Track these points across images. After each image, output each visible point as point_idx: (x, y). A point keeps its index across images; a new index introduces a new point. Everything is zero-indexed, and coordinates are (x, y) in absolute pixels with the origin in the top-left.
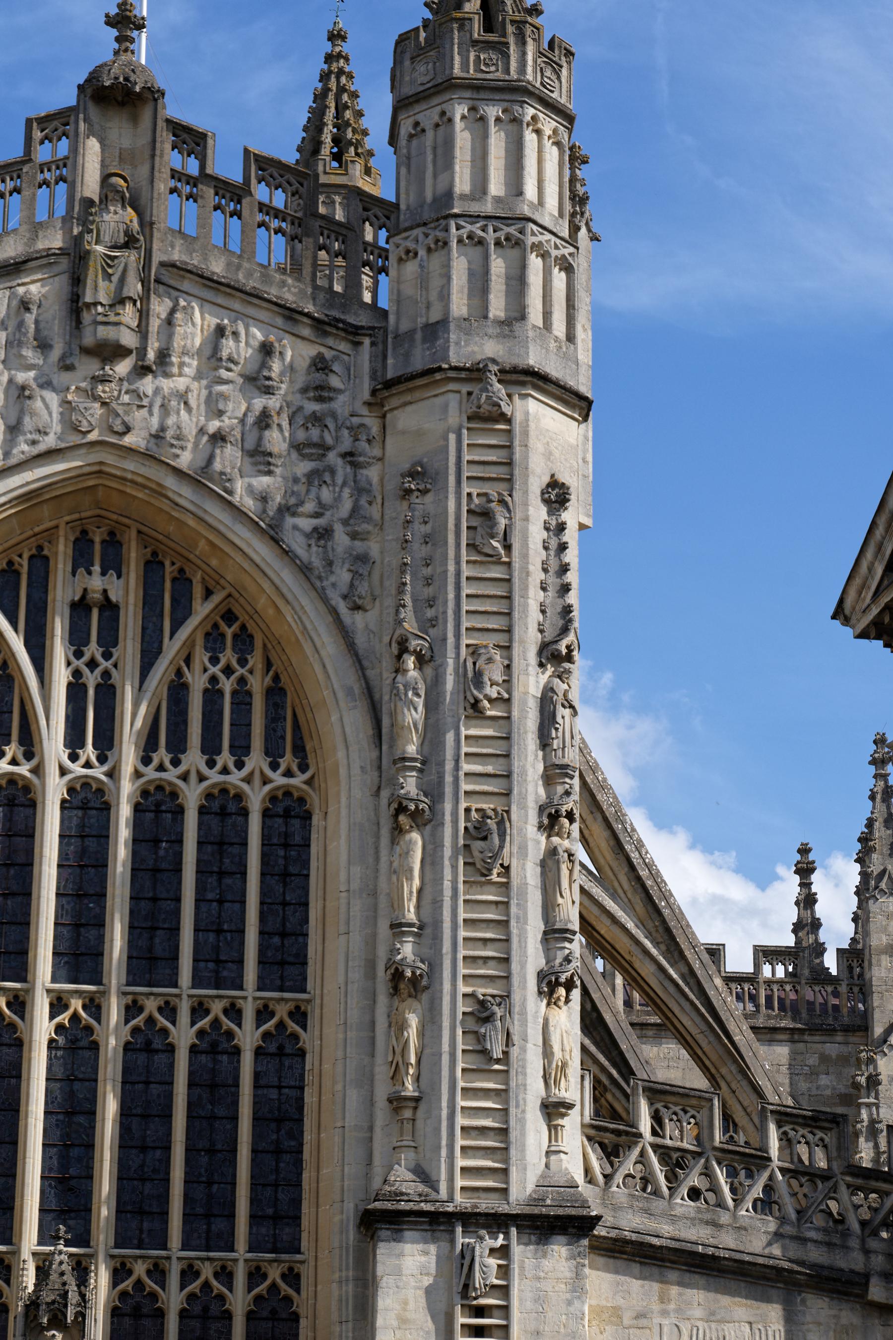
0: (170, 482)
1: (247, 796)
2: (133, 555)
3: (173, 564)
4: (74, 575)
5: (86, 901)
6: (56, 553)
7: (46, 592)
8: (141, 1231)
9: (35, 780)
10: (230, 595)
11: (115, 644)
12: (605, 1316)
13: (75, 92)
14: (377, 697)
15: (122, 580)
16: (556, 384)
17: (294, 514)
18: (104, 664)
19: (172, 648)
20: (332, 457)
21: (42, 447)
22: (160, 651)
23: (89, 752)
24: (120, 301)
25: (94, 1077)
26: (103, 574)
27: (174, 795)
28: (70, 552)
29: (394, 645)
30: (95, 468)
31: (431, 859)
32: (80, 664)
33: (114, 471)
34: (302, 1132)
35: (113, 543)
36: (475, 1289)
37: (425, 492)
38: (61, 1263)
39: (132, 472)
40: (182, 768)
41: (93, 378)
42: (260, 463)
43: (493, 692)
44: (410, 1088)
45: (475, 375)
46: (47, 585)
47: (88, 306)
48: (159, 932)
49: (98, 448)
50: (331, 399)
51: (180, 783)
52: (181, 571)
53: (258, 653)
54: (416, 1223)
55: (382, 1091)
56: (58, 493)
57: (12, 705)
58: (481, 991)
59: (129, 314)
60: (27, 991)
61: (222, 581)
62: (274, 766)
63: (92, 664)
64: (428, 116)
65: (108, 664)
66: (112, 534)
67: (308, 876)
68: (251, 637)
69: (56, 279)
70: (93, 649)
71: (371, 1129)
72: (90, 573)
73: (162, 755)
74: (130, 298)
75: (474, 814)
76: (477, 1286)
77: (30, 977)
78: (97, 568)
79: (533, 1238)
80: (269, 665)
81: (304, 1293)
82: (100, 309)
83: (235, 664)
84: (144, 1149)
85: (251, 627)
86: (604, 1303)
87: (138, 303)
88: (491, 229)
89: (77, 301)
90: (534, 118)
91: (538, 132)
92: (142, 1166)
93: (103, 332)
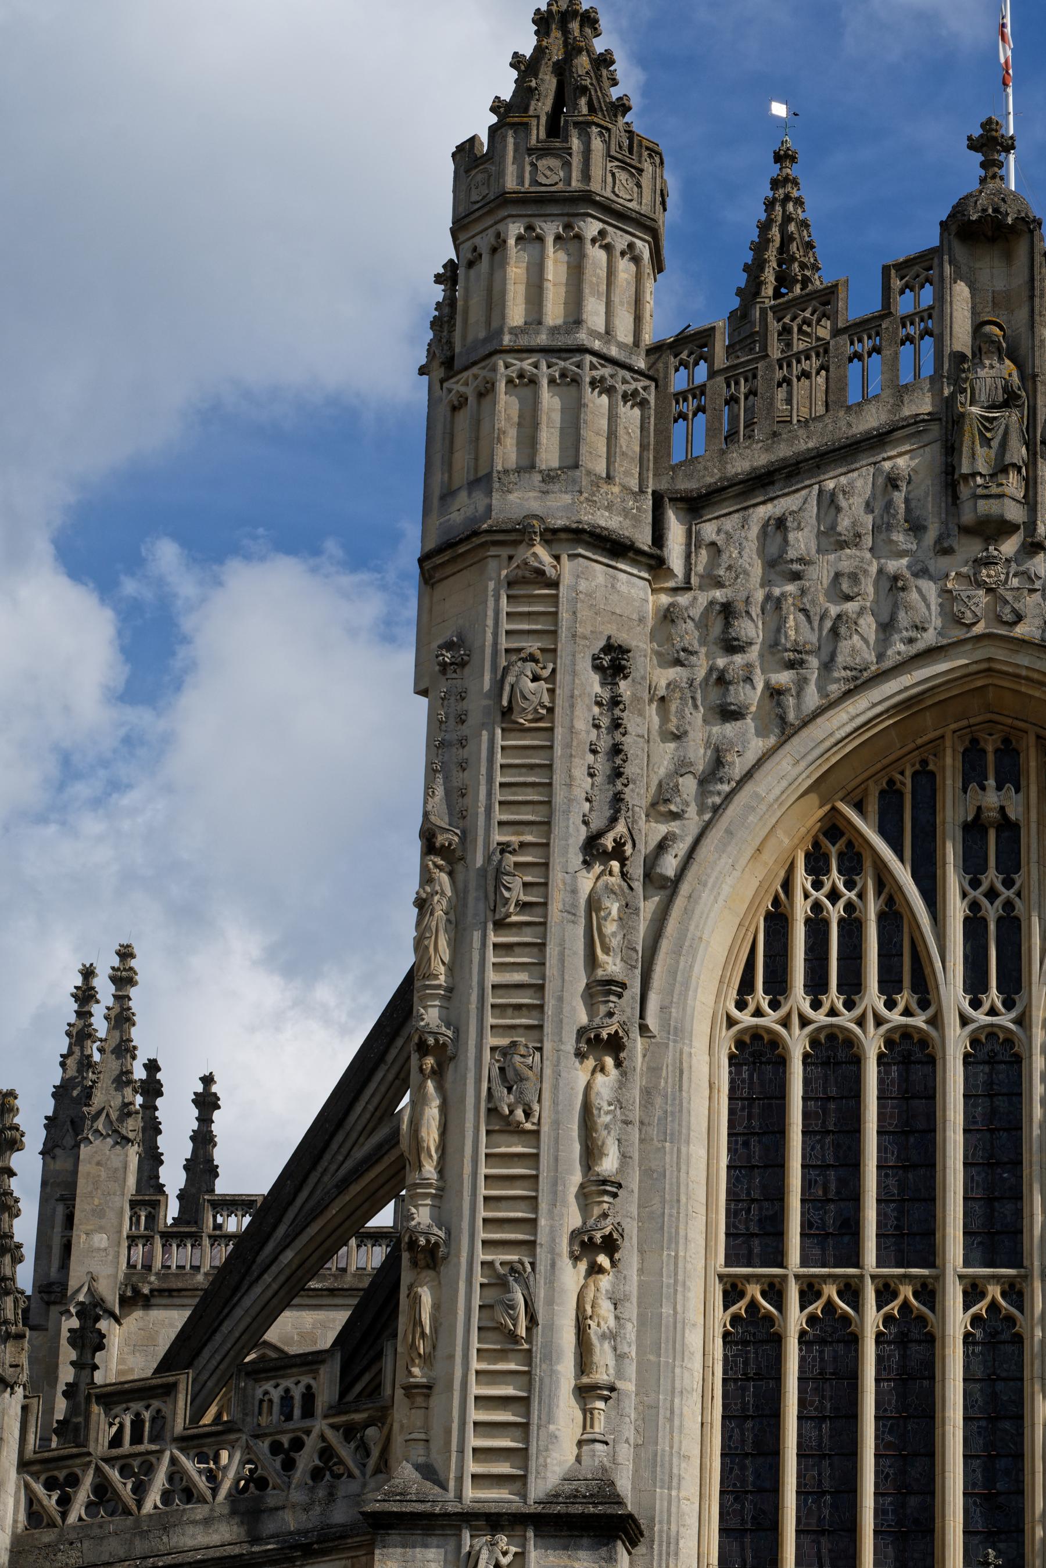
2: (1033, 764)
4: (965, 792)
5: (999, 1171)
6: (944, 768)
7: (934, 813)
9: (933, 1033)
11: (1017, 869)
13: (937, 230)
15: (1021, 795)
18: (1006, 893)
21: (920, 646)
23: (994, 996)
24: (1002, 469)
26: (999, 788)
28: (959, 765)
30: (984, 666)
32: (977, 894)
33: (1005, 668)
35: (1009, 753)
39: (1027, 668)
41: (975, 561)
46: (935, 806)
47: (965, 477)
49: (985, 643)
56: (942, 698)
57: (901, 946)
59: (1013, 485)
63: (992, 894)
65: (1010, 893)
66: (1006, 741)
69: (927, 449)
70: (992, 876)
72: (983, 788)
74: (1014, 465)
77: (938, 1262)
78: (991, 782)
82: (979, 480)
87: (1024, 470)
89: (953, 473)
93: (983, 506)
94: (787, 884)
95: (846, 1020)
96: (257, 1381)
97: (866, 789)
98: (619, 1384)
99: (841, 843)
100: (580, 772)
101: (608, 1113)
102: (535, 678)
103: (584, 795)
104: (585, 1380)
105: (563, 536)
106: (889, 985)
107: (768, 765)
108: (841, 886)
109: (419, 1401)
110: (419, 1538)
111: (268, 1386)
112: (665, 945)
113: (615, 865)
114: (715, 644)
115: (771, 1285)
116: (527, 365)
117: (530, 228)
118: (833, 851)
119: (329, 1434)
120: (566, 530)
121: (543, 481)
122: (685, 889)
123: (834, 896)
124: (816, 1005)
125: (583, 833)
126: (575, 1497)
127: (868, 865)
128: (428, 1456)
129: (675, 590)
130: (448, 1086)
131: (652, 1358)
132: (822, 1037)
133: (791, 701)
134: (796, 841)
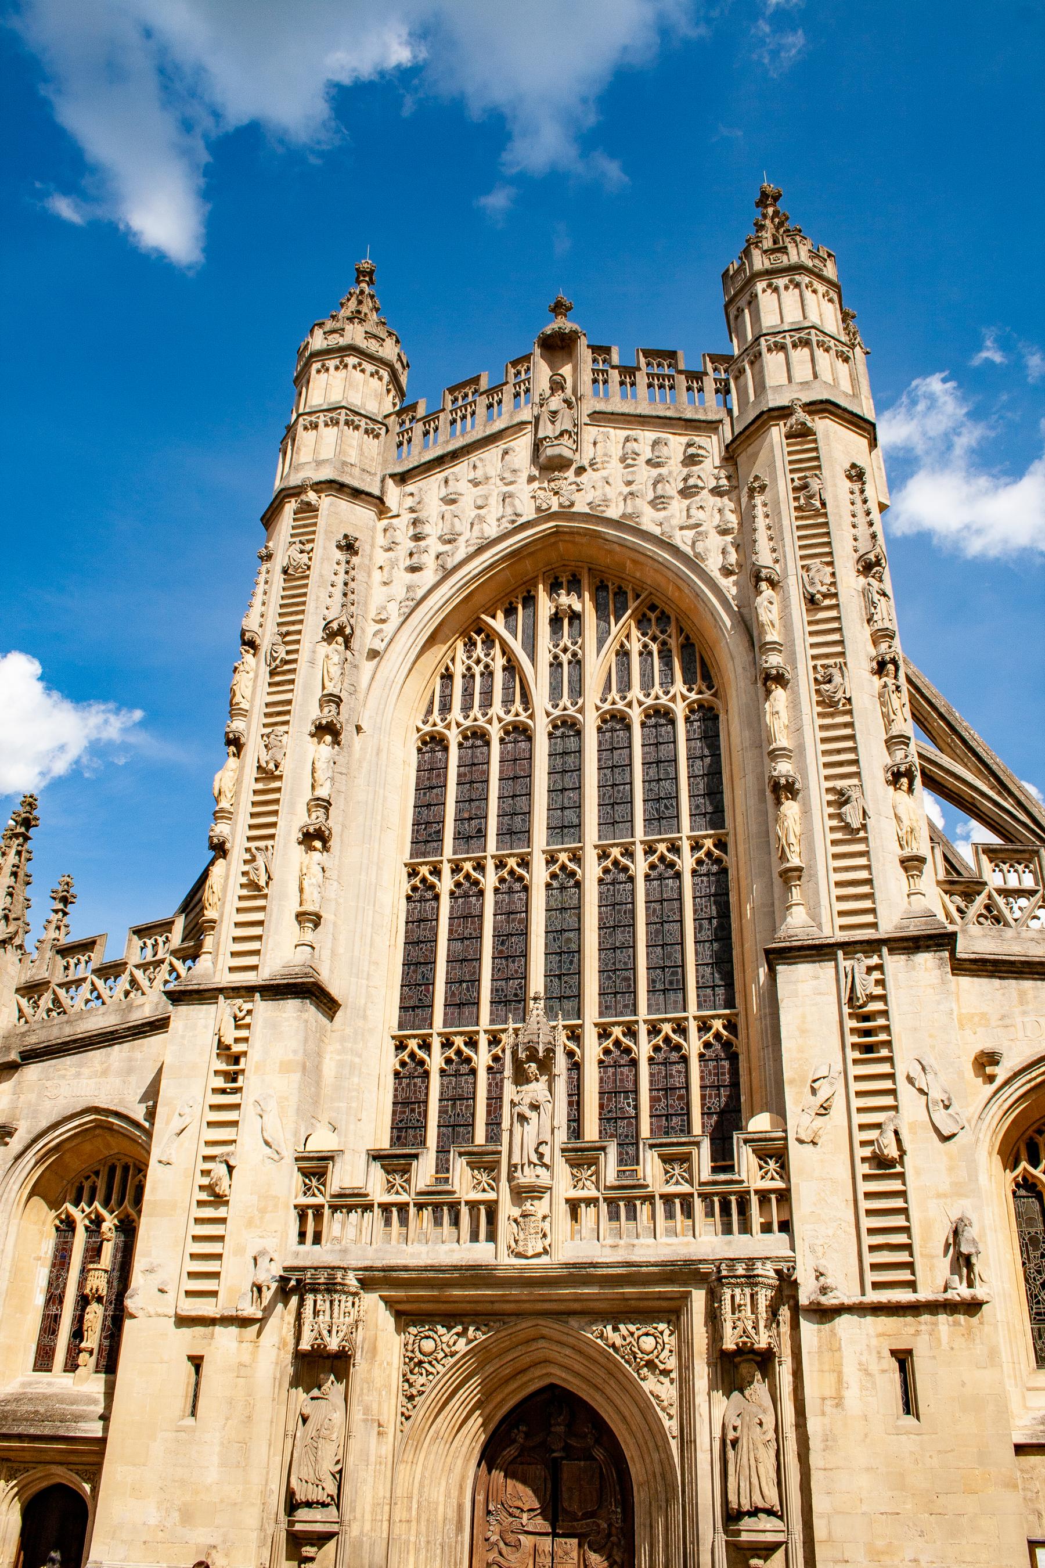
1: (672, 710)
10: (651, 593)
12: (976, 1019)
14: (748, 623)
16: (845, 410)
17: (682, 528)
19: (614, 630)
20: (705, 492)
23: (565, 701)
26: (568, 594)
29: (753, 579)
31: (795, 705)
34: (730, 925)
36: (858, 999)
37: (763, 488)
38: (538, 1015)
43: (824, 589)
44: (795, 861)
45: (786, 412)
50: (701, 462)
51: (627, 709)
52: (620, 588)
53: (673, 623)
54: (806, 956)
55: (775, 875)
58: (839, 784)
62: (690, 690)
64: (742, 302)
66: (574, 575)
67: (720, 755)
68: (668, 617)
70: (566, 641)
71: (773, 904)
72: (558, 595)
73: (614, 694)
75: (819, 668)
76: (859, 995)
79: (903, 957)
80: (681, 630)
81: (740, 1037)
83: (658, 633)
85: (667, 609)
86: (974, 1011)
88: (788, 337)
90: (810, 282)
91: (815, 291)
100: (323, 595)
102: (302, 552)
106: (507, 702)
108: (482, 656)
113: (340, 639)
116: (313, 418)
117: (323, 366)
122: (386, 657)
123: (478, 662)
124: (466, 717)
133: (449, 560)
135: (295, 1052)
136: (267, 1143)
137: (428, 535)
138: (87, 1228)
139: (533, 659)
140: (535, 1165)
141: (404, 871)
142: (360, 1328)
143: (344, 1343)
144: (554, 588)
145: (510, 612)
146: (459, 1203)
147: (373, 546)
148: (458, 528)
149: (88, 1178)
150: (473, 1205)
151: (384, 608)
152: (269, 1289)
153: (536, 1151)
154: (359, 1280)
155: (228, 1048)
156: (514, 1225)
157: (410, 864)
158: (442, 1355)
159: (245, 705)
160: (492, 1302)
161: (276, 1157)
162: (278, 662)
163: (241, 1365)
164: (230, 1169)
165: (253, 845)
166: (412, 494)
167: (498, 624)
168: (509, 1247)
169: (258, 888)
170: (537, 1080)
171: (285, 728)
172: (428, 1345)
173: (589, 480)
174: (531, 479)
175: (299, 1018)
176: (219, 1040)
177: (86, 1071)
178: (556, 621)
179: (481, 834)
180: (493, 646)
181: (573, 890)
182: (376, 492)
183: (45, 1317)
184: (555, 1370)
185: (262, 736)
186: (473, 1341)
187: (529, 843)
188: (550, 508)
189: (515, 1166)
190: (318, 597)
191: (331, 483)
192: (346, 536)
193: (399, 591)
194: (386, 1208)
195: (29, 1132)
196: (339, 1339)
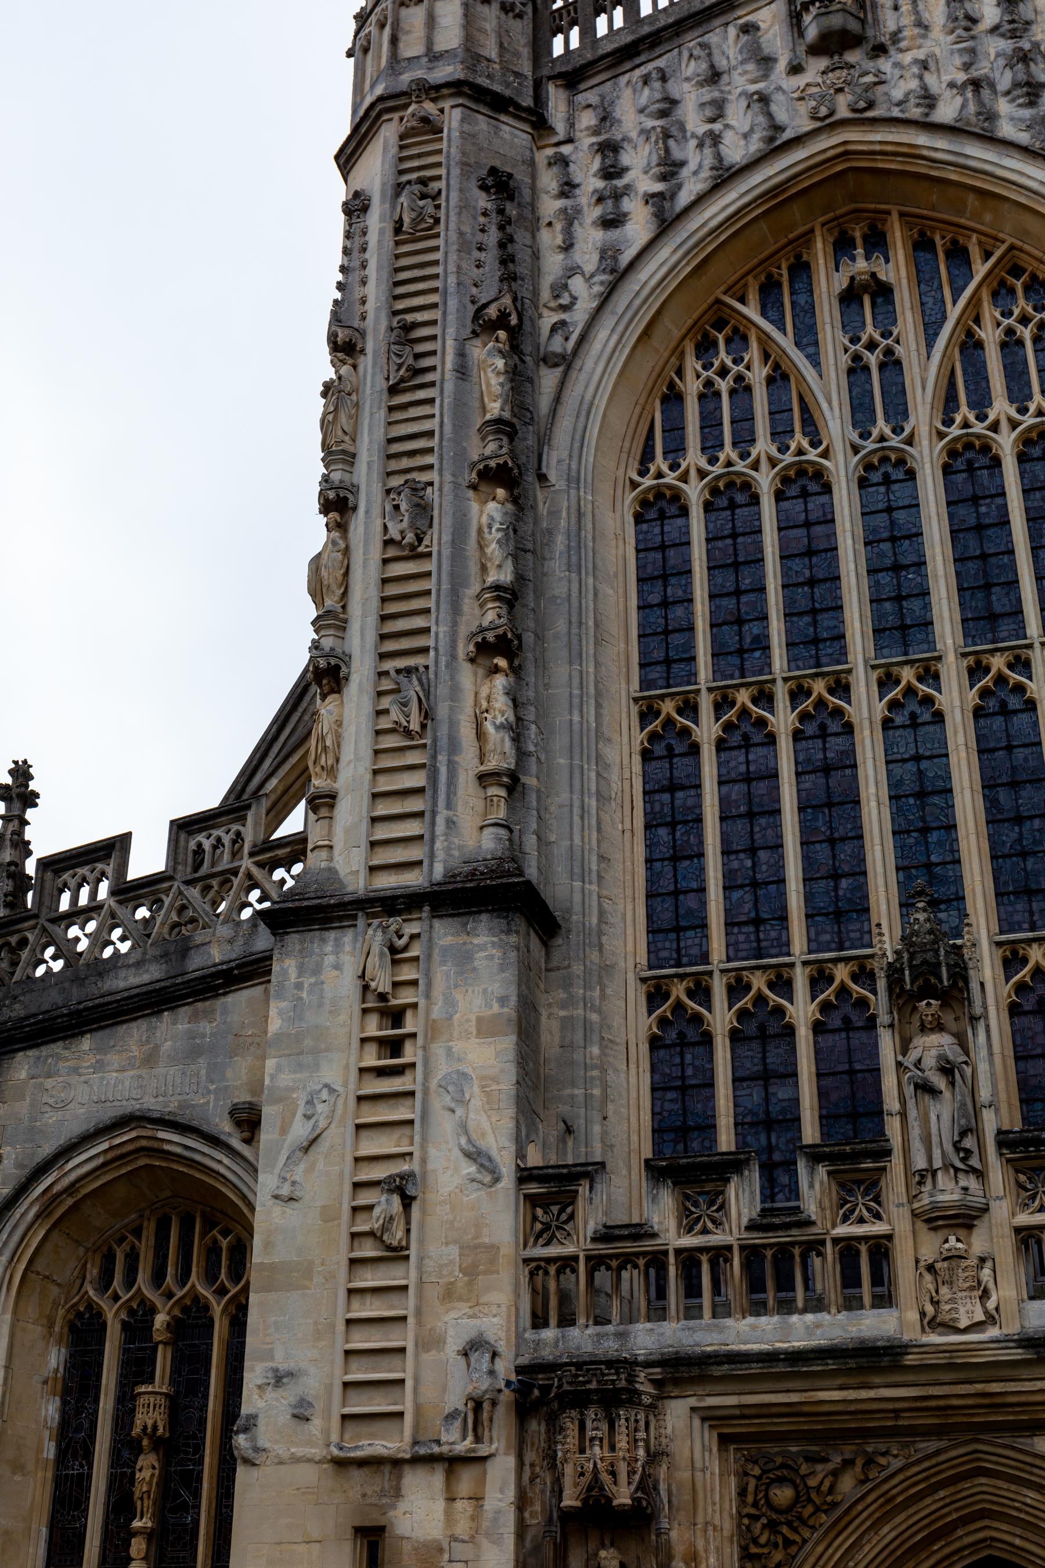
0: (922, 139)
2: (898, 234)
3: (943, 238)
5: (904, 573)
8: (1031, 913)
10: (1012, 247)
11: (894, 322)
15: (891, 265)
22: (944, 318)
23: (881, 426)
25: (943, 752)
26: (867, 258)
27: (986, 449)
28: (830, 250)
40: (992, 417)
42: (1019, 97)
48: (994, 590)
52: (954, 242)
60: (849, 671)
61: (1001, 235)
66: (873, 227)
70: (870, 331)
72: (853, 259)
73: (964, 412)
78: (860, 251)
84: (1019, 820)
92: (1020, 839)
94: (680, 372)
95: (740, 466)
96: (190, 833)
97: (746, 285)
98: (524, 779)
99: (728, 330)
101: (498, 530)
102: (423, 196)
103: (471, 282)
104: (482, 768)
105: (445, 91)
106: (780, 434)
107: (647, 257)
108: (729, 362)
109: (324, 812)
110: (317, 933)
111: (201, 838)
112: (561, 411)
113: (502, 334)
114: (595, 175)
115: (686, 702)
118: (721, 338)
119: (255, 871)
120: (447, 85)
121: (430, 61)
123: (723, 372)
124: (713, 460)
125: (471, 309)
126: (474, 875)
127: (754, 345)
128: (331, 859)
129: (558, 144)
130: (351, 534)
131: (562, 761)
132: (721, 485)
133: (667, 205)
134: (684, 331)
135: (503, 1000)
136: (468, 1155)
137: (625, 170)
138: (125, 1326)
139: (816, 363)
140: (957, 1170)
141: (635, 710)
142: (664, 1467)
143: (639, 1494)
144: (843, 247)
145: (769, 291)
146: (823, 1243)
147: (533, 188)
148: (677, 154)
149: (123, 1239)
150: (848, 1248)
151: (566, 286)
152: (494, 1403)
153: (957, 1147)
154: (657, 1383)
155: (383, 997)
156: (928, 1277)
157: (643, 698)
158: (810, 1509)
159: (347, 446)
160: (896, 1412)
161: (487, 1178)
162: (402, 372)
163: (454, 1538)
164: (407, 1202)
165: (390, 665)
166: (589, 106)
167: (751, 311)
168: (923, 1314)
169: (408, 733)
170: (939, 1027)
171: (424, 477)
172: (783, 1495)
173: (897, 65)
174: (795, 69)
175: (502, 945)
176: (366, 988)
177: (114, 1059)
178: (850, 297)
179: (762, 644)
180: (747, 347)
181: (930, 728)
182: (527, 101)
183: (59, 1481)
184: (1003, 1531)
185: (388, 492)
186: (863, 1482)
187: (842, 655)
188: (831, 114)
189: (922, 1175)
190: (459, 267)
191: (457, 87)
192: (493, 171)
193: (587, 255)
194: (689, 1259)
195: (19, 1165)
196: (633, 1487)
